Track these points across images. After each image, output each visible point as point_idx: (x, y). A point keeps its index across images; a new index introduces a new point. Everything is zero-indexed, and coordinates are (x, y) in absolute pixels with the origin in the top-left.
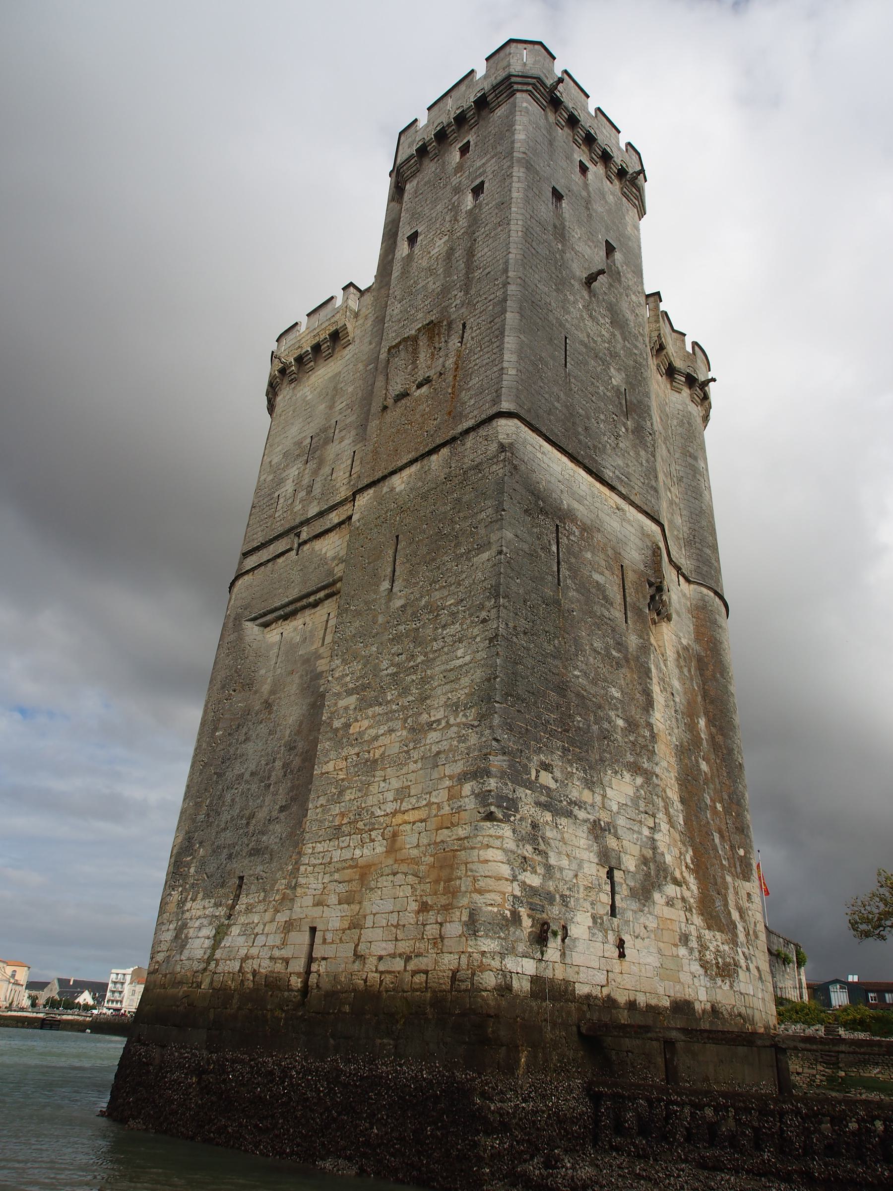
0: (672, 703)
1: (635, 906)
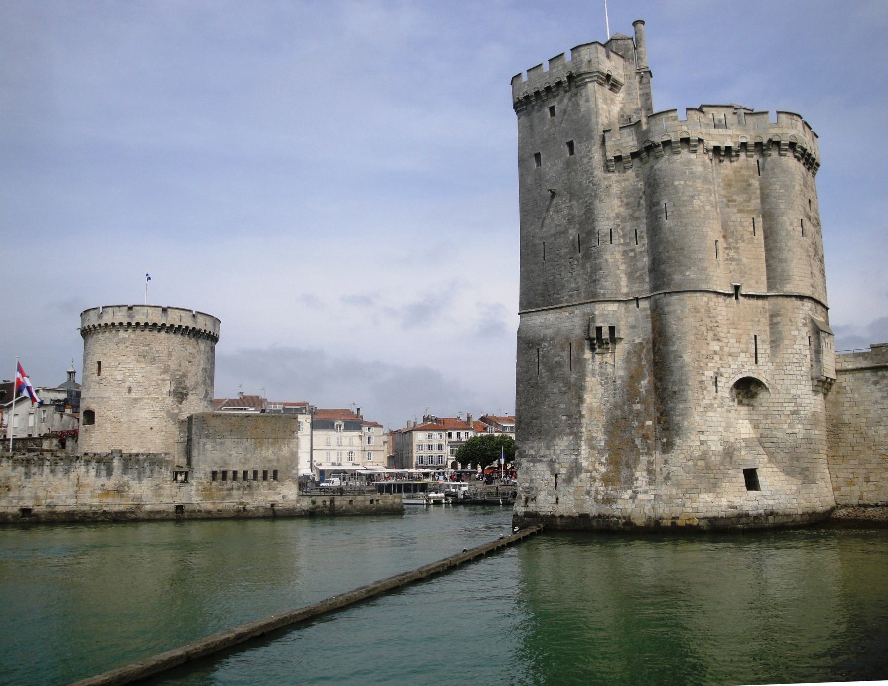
0: (612, 387)
1: (565, 485)
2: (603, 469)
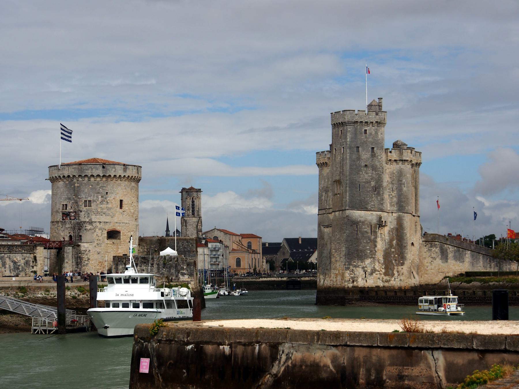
2: (383, 271)
